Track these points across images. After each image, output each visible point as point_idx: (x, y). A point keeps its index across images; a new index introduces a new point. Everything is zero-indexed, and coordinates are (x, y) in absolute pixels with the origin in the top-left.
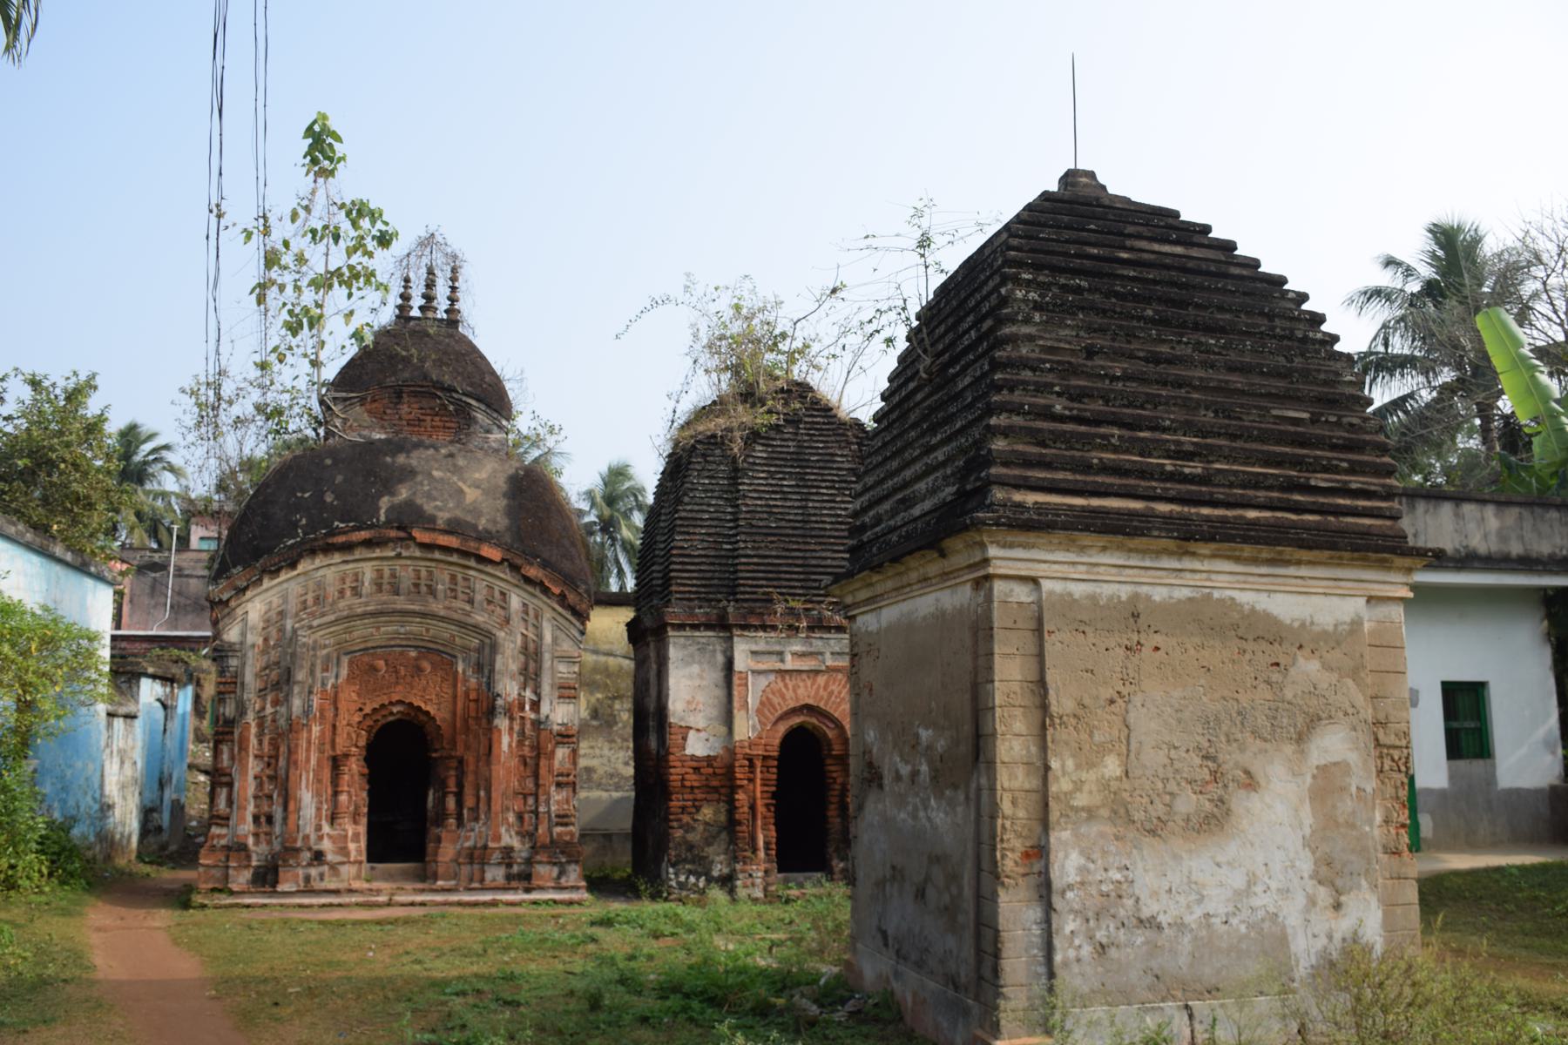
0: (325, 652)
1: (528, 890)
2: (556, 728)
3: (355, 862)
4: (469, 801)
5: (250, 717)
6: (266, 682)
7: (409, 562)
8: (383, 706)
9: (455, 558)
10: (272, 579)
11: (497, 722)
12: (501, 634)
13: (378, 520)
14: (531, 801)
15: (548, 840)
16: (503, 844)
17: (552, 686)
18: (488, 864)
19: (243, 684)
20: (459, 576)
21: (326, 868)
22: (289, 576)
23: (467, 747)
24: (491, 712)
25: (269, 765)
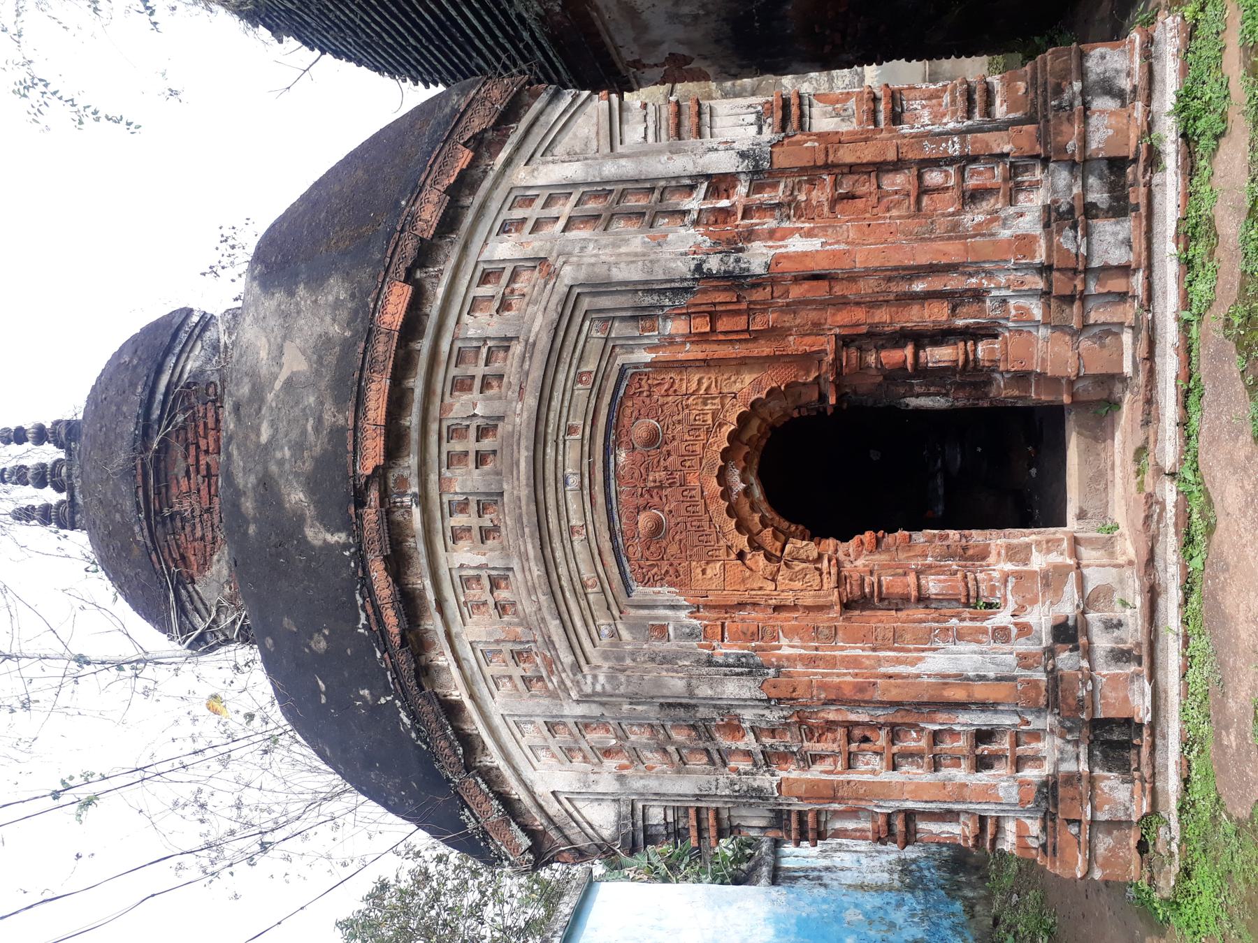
0: (625, 635)
1: (1154, 159)
2: (768, 135)
3: (1075, 554)
4: (937, 314)
5: (765, 781)
6: (693, 751)
7: (433, 477)
8: (731, 511)
9: (416, 384)
10: (484, 748)
11: (757, 267)
12: (568, 275)
13: (346, 546)
14: (934, 178)
15: (1030, 128)
16: (1038, 230)
17: (677, 151)
18: (1088, 258)
19: (698, 797)
20: (454, 371)
21: (1092, 616)
22: (475, 716)
23: (817, 328)
24: (736, 281)
25: (866, 739)
